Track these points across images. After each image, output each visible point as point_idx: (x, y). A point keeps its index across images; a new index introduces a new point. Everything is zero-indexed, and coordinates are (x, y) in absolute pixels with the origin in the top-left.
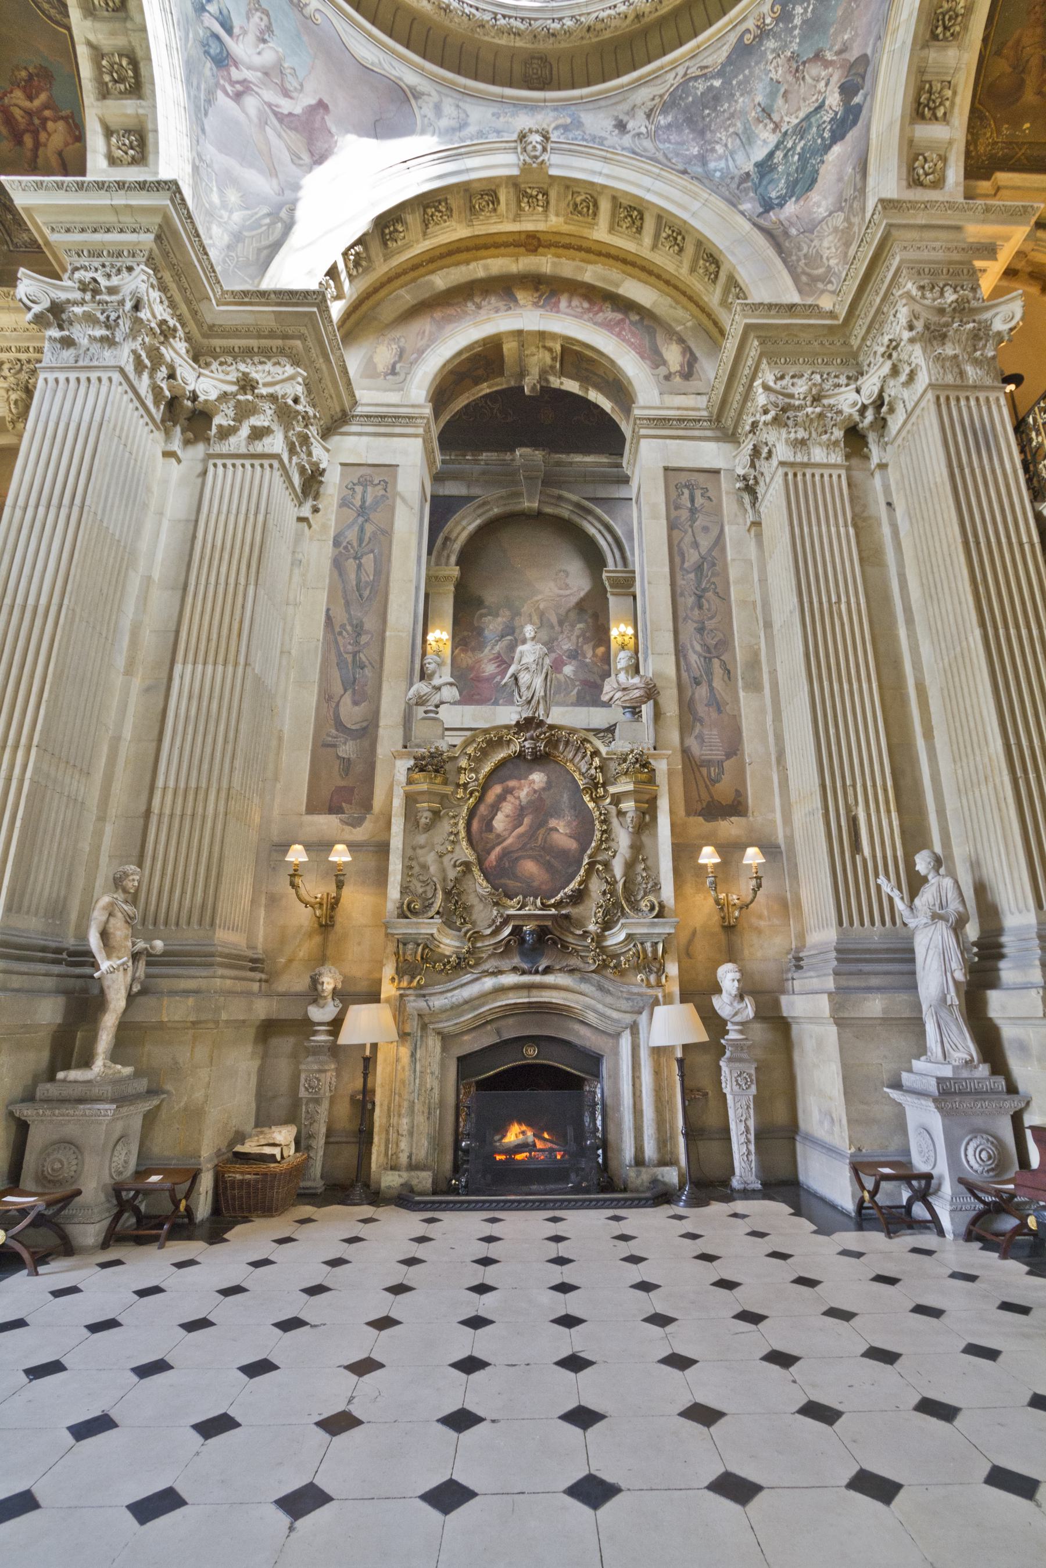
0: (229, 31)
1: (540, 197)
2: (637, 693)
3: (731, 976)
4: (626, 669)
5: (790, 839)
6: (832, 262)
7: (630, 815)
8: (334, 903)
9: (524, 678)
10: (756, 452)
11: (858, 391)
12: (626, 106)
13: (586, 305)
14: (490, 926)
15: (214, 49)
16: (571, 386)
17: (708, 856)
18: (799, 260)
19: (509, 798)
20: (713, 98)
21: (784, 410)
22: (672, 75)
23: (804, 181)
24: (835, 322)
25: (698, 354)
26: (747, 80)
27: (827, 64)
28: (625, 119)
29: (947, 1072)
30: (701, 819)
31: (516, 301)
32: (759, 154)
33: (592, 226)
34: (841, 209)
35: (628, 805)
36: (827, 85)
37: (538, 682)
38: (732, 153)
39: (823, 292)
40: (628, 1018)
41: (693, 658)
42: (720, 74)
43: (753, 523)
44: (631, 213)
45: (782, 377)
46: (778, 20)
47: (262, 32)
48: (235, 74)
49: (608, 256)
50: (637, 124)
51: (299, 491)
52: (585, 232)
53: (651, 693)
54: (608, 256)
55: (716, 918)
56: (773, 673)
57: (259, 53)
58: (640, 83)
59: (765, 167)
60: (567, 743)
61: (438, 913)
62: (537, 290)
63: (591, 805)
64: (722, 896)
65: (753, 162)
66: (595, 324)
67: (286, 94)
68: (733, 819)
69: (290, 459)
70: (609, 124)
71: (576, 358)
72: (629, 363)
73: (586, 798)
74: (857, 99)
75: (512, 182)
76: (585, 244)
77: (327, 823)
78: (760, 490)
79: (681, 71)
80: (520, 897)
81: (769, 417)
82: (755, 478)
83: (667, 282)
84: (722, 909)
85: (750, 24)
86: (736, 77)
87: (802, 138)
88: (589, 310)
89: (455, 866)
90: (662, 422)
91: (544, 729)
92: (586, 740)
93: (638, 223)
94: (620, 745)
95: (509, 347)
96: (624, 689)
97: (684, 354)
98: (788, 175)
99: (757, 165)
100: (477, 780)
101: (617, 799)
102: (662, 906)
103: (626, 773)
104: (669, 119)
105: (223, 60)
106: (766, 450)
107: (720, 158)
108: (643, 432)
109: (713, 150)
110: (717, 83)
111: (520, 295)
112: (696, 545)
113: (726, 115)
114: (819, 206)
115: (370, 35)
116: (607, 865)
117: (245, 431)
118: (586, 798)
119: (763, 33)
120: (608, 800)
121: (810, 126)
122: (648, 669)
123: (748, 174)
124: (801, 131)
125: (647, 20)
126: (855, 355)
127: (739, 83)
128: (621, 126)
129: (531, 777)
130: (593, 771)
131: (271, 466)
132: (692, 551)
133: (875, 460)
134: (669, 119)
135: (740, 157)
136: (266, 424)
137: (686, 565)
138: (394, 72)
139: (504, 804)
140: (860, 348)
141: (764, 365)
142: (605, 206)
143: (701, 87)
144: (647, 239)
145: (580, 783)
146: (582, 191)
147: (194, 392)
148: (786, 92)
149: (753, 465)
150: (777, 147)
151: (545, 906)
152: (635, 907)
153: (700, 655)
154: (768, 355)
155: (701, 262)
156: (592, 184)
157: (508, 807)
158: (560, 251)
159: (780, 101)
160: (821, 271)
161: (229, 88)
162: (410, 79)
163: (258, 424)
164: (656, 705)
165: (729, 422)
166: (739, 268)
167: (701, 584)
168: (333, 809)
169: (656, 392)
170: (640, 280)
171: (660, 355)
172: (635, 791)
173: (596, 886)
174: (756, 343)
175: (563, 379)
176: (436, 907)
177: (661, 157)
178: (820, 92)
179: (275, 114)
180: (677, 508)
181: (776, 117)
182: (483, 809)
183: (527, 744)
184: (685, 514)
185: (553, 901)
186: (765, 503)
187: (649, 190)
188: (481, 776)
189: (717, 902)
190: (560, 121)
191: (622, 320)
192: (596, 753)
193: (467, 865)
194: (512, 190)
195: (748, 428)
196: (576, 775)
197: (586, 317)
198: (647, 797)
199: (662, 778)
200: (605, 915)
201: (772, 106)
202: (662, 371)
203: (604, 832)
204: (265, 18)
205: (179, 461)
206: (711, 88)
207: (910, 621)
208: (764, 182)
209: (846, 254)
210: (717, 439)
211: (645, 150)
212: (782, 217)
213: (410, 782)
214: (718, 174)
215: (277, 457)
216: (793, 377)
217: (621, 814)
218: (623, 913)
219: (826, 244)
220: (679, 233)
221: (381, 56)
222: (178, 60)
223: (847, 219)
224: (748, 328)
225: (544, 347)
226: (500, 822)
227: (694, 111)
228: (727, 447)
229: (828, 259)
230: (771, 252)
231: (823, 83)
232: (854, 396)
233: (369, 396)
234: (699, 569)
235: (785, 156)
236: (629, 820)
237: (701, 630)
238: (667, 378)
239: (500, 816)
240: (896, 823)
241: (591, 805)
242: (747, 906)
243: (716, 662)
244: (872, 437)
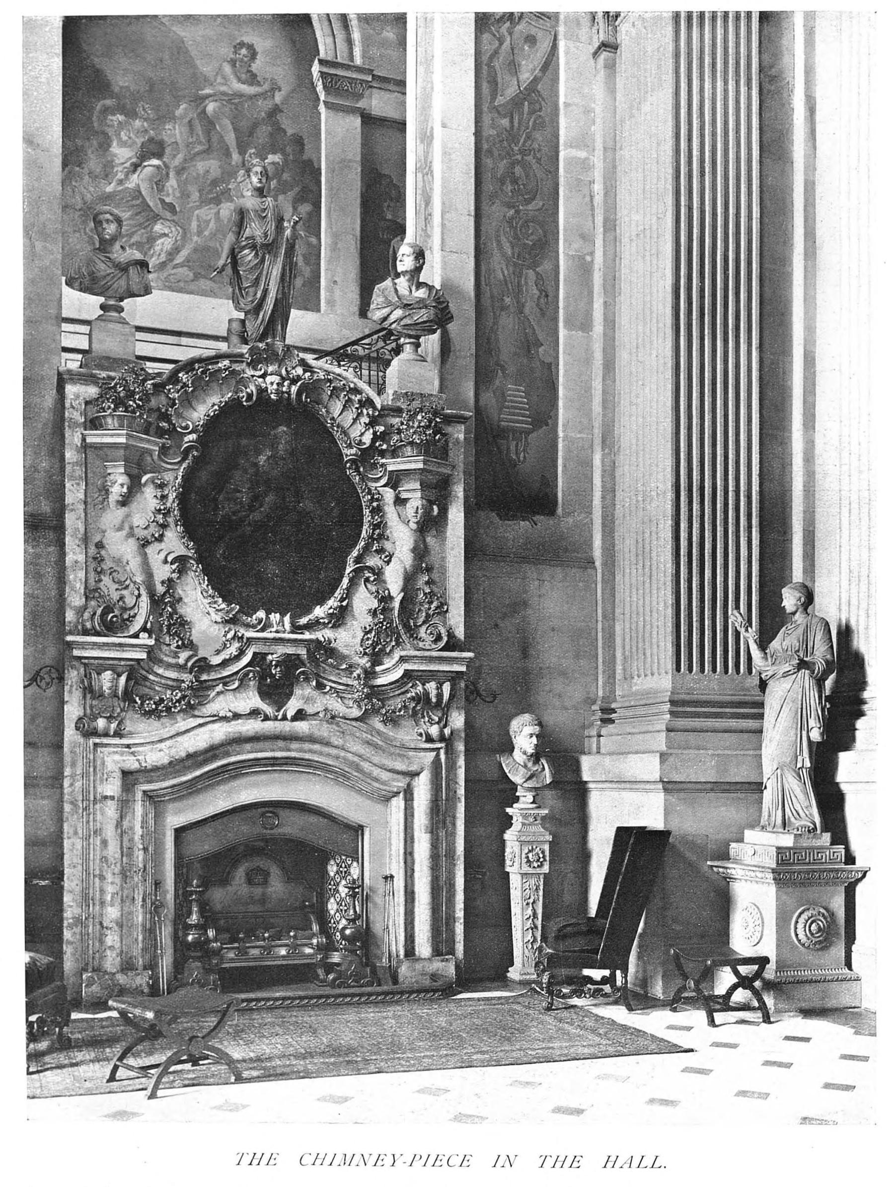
61: (144, 629)
89: (165, 561)
101: (395, 480)
116: (378, 573)
120: (383, 481)
132: (507, 77)
137: (500, 100)
151: (296, 628)
203: (376, 526)
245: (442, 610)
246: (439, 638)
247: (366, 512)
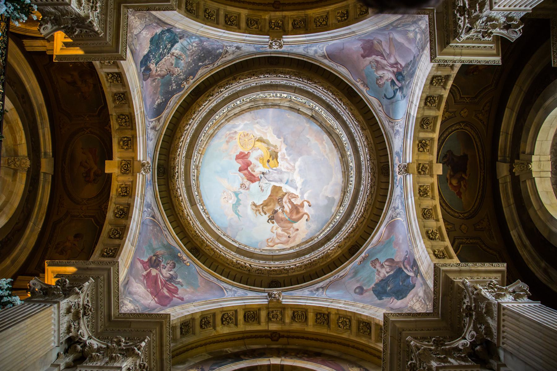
12: (236, 53)
15: (400, 77)
20: (200, 59)
26: (189, 66)
28: (237, 50)
42: (201, 66)
46: (181, 84)
50: (230, 50)
70: (243, 49)
76: (251, 6)
79: (216, 66)
93: (227, 19)
104: (218, 51)
107: (194, 42)
110: (200, 64)
115: (340, 74)
119: (186, 79)
125: (231, 78)
134: (218, 51)
142: (243, 25)
143: (207, 62)
144: (222, 13)
206: (202, 62)
208: (172, 37)
220: (207, 18)
221: (336, 68)
222: (415, 80)
235: (166, 46)
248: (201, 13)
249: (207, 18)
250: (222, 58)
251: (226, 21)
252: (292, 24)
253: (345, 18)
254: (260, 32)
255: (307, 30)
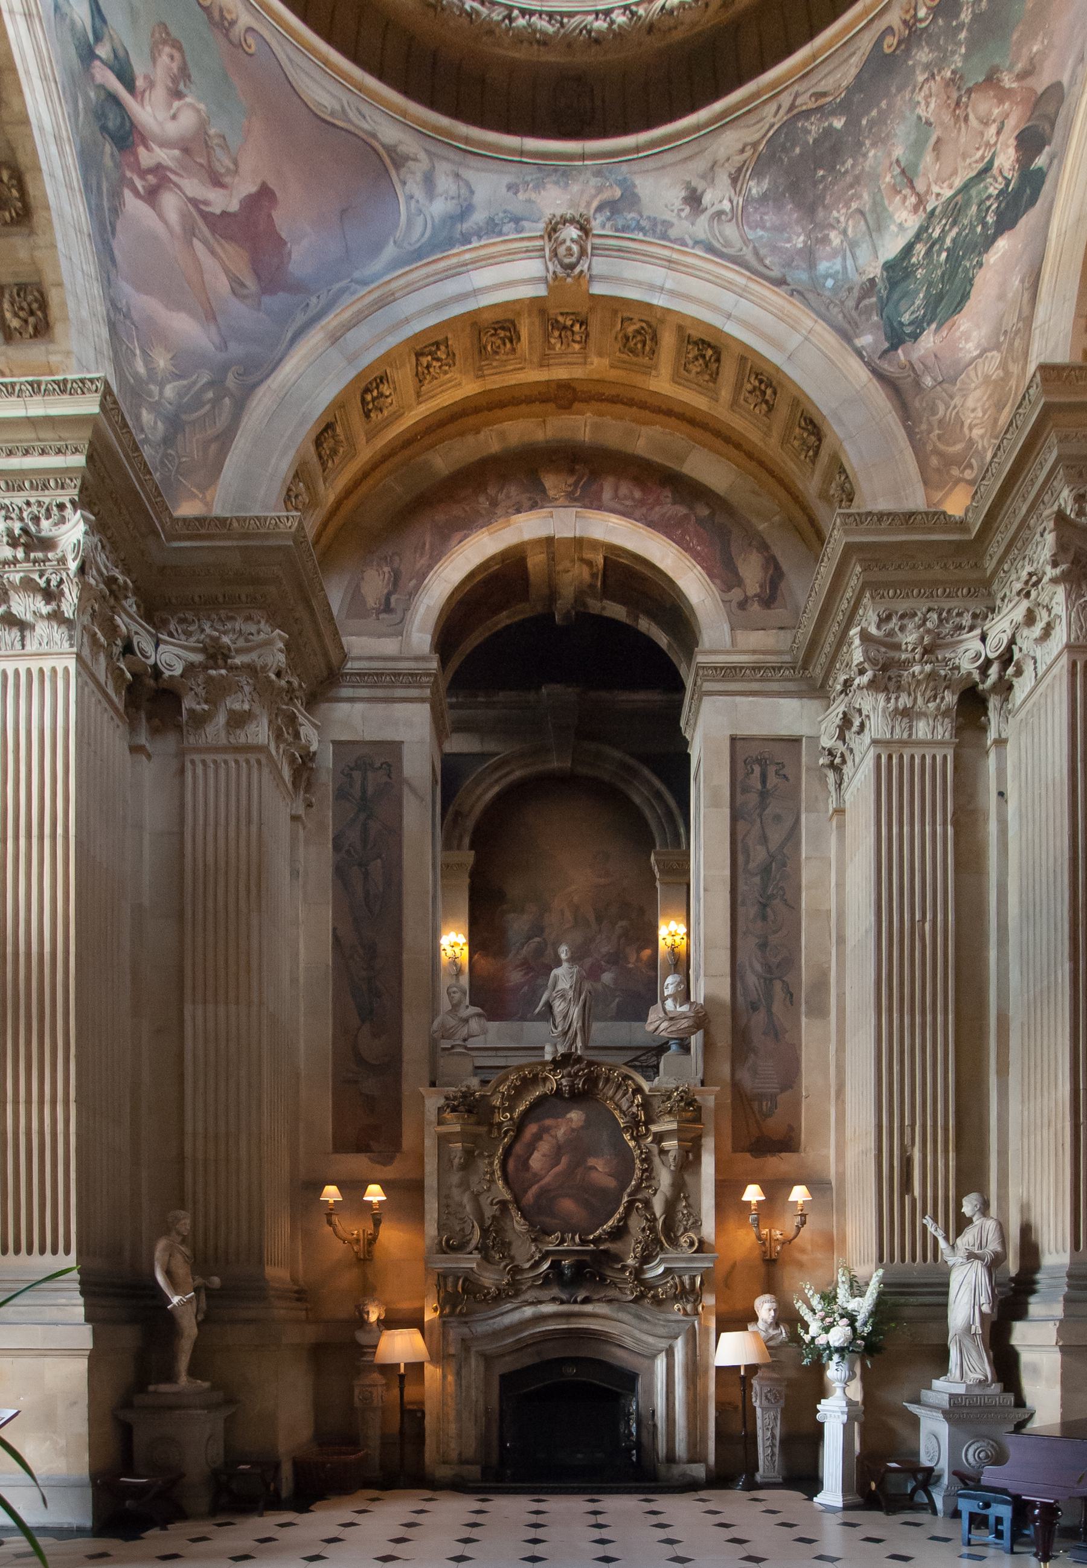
0: (128, 82)
1: (577, 328)
2: (684, 1024)
3: (767, 1306)
4: (674, 997)
5: (841, 1176)
6: (977, 432)
7: (672, 1154)
8: (372, 1240)
9: (559, 1007)
10: (846, 722)
11: (983, 638)
13: (637, 494)
14: (529, 1260)
16: (616, 611)
17: (753, 1194)
18: (930, 432)
19: (545, 1136)
20: (831, 151)
21: (885, 668)
22: (772, 107)
23: (950, 296)
24: (966, 537)
25: (785, 568)
27: (1003, 95)
29: (961, 1389)
30: (748, 1155)
31: (544, 491)
32: (891, 247)
33: (648, 370)
34: (997, 347)
35: (671, 1144)
36: (998, 133)
37: (575, 1012)
38: (853, 245)
39: (958, 481)
40: (663, 1344)
41: (752, 980)
42: (844, 107)
43: (836, 811)
44: (705, 350)
45: (889, 618)
47: (175, 80)
48: (146, 159)
49: (669, 413)
51: (290, 786)
52: (638, 380)
53: (702, 1021)
54: (669, 413)
55: (757, 1253)
56: (841, 996)
57: (174, 117)
58: (724, 122)
59: (898, 270)
60: (607, 1080)
61: (476, 1248)
62: (572, 471)
63: (632, 1144)
64: (765, 1231)
65: (882, 261)
66: (651, 524)
67: (217, 181)
68: (783, 1155)
69: (278, 747)
71: (628, 577)
72: (692, 582)
73: (627, 1137)
74: (1040, 161)
75: (537, 306)
77: (356, 1163)
78: (847, 770)
79: (786, 99)
80: (558, 1234)
81: (865, 679)
82: (842, 755)
83: (750, 456)
84: (764, 1244)
85: (894, 18)
86: (867, 112)
87: (954, 223)
88: (642, 503)
89: (492, 1204)
90: (731, 672)
91: (583, 1066)
92: (626, 1077)
94: (665, 1080)
95: (536, 561)
96: (671, 1019)
97: (765, 568)
98: (930, 285)
99: (889, 266)
100: (512, 1119)
101: (659, 1138)
102: (701, 1242)
103: (670, 1112)
105: (125, 135)
106: (857, 723)
108: (708, 686)
109: (825, 240)
110: (838, 123)
111: (551, 482)
112: (764, 839)
113: (849, 179)
114: (967, 340)
116: (648, 1204)
117: (221, 719)
118: (627, 1137)
120: (650, 1139)
121: (967, 204)
122: (698, 994)
123: (872, 281)
124: (954, 210)
126: (987, 583)
127: (872, 123)
128: (694, 199)
129: (568, 1116)
130: (634, 1109)
131: (259, 762)
132: (759, 847)
133: (992, 735)
135: (863, 252)
136: (246, 707)
137: (752, 866)
138: (366, 126)
139: (541, 1143)
140: (995, 572)
141: (866, 600)
143: (814, 128)
145: (621, 1121)
146: (636, 317)
147: (155, 666)
148: (939, 140)
149: (842, 737)
150: (918, 237)
151: (584, 1242)
152: (674, 1242)
153: (759, 976)
154: (872, 587)
155: (797, 430)
156: (650, 306)
157: (544, 1147)
158: (604, 406)
159: (928, 158)
160: (959, 447)
161: (139, 184)
162: (389, 133)
163: (237, 706)
164: (707, 1035)
165: (818, 670)
166: (847, 446)
167: (766, 897)
168: (361, 1147)
169: (726, 627)
170: (711, 449)
171: (737, 574)
172: (679, 1130)
173: (637, 1223)
174: (858, 569)
175: (607, 603)
176: (474, 1243)
177: (748, 254)
178: (988, 145)
179: (205, 215)
180: (745, 790)
181: (920, 186)
182: (518, 1148)
183: (564, 1082)
184: (753, 798)
185: (591, 1237)
186: (850, 790)
187: (729, 316)
188: (516, 1115)
189: (759, 1238)
190: (605, 195)
191: (686, 517)
192: (638, 1090)
193: (503, 1204)
194: (537, 321)
195: (839, 687)
196: (617, 1113)
197: (638, 513)
198: (693, 1135)
199: (708, 1117)
200: (643, 1250)
201: (916, 166)
202: (736, 594)
203: (644, 1171)
204: (177, 55)
205: (149, 757)
206: (829, 131)
207: (1003, 942)
209: (996, 421)
210: (798, 695)
211: (728, 244)
212: (915, 356)
213: (440, 1123)
214: (830, 283)
215: (262, 749)
216: (902, 617)
217: (663, 1152)
218: (662, 1248)
219: (970, 403)
223: (1003, 365)
224: (850, 549)
225: (582, 560)
226: (536, 1161)
227: (804, 169)
228: (812, 705)
229: (970, 429)
230: (893, 420)
231: (993, 129)
232: (977, 645)
233: (364, 646)
234: (766, 871)
236: (671, 1159)
237: (763, 946)
238: (743, 605)
239: (536, 1155)
240: (952, 1163)
241: (632, 1144)
242: (790, 1241)
243: (778, 986)
244: (993, 702)
245: (697, 1225)
246: (692, 1244)
247: (637, 1161)
248: (783, 411)
249: (769, 385)
250: (755, 145)
251: (718, 360)
252: (519, 339)
253: (369, 397)
254: (616, 306)
255: (474, 324)
